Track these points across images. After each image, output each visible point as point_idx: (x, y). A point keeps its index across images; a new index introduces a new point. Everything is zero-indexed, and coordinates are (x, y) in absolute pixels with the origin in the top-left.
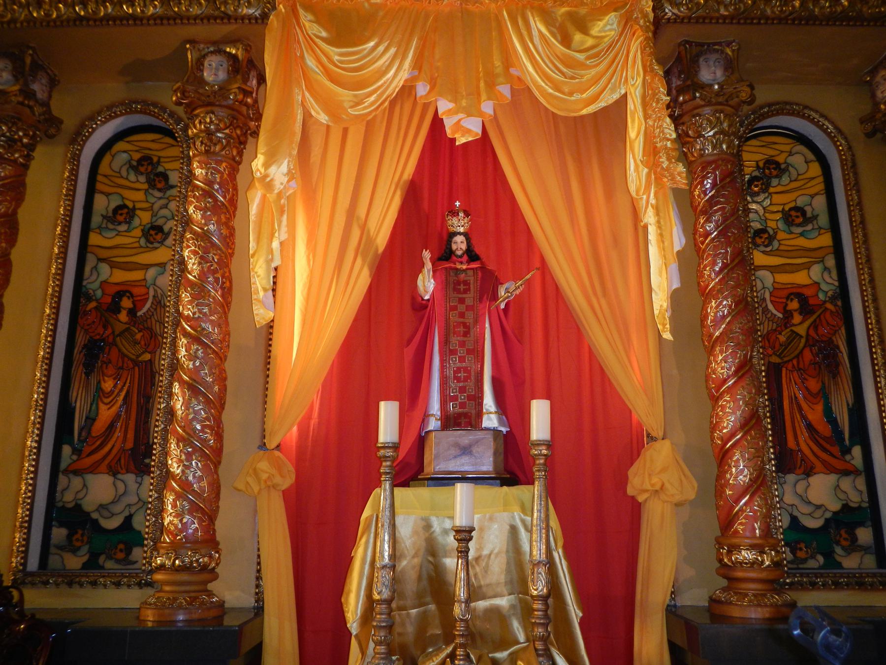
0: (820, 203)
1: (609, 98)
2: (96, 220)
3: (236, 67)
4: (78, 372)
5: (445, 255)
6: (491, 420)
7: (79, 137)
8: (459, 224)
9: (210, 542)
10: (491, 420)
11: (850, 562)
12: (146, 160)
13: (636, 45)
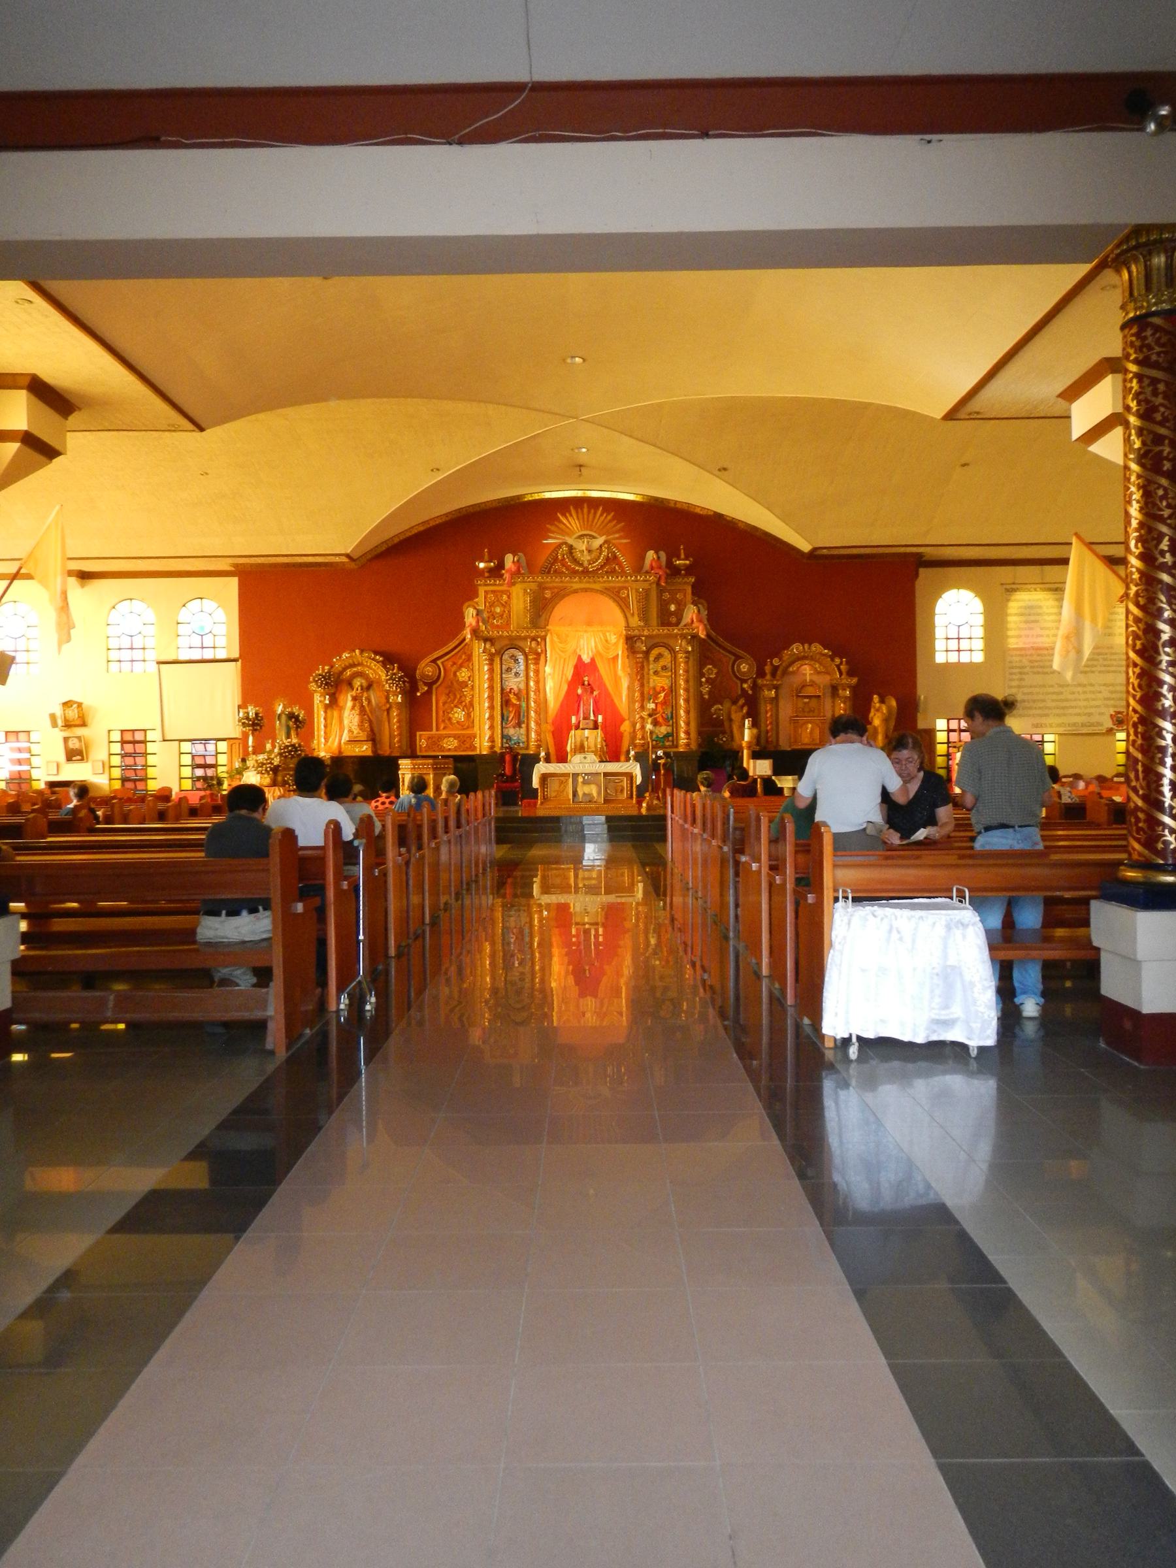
0: (670, 664)
1: (615, 654)
2: (503, 671)
3: (538, 644)
4: (504, 707)
5: (583, 685)
6: (592, 717)
7: (500, 652)
8: (586, 679)
9: (540, 741)
10: (592, 717)
11: (667, 744)
12: (513, 656)
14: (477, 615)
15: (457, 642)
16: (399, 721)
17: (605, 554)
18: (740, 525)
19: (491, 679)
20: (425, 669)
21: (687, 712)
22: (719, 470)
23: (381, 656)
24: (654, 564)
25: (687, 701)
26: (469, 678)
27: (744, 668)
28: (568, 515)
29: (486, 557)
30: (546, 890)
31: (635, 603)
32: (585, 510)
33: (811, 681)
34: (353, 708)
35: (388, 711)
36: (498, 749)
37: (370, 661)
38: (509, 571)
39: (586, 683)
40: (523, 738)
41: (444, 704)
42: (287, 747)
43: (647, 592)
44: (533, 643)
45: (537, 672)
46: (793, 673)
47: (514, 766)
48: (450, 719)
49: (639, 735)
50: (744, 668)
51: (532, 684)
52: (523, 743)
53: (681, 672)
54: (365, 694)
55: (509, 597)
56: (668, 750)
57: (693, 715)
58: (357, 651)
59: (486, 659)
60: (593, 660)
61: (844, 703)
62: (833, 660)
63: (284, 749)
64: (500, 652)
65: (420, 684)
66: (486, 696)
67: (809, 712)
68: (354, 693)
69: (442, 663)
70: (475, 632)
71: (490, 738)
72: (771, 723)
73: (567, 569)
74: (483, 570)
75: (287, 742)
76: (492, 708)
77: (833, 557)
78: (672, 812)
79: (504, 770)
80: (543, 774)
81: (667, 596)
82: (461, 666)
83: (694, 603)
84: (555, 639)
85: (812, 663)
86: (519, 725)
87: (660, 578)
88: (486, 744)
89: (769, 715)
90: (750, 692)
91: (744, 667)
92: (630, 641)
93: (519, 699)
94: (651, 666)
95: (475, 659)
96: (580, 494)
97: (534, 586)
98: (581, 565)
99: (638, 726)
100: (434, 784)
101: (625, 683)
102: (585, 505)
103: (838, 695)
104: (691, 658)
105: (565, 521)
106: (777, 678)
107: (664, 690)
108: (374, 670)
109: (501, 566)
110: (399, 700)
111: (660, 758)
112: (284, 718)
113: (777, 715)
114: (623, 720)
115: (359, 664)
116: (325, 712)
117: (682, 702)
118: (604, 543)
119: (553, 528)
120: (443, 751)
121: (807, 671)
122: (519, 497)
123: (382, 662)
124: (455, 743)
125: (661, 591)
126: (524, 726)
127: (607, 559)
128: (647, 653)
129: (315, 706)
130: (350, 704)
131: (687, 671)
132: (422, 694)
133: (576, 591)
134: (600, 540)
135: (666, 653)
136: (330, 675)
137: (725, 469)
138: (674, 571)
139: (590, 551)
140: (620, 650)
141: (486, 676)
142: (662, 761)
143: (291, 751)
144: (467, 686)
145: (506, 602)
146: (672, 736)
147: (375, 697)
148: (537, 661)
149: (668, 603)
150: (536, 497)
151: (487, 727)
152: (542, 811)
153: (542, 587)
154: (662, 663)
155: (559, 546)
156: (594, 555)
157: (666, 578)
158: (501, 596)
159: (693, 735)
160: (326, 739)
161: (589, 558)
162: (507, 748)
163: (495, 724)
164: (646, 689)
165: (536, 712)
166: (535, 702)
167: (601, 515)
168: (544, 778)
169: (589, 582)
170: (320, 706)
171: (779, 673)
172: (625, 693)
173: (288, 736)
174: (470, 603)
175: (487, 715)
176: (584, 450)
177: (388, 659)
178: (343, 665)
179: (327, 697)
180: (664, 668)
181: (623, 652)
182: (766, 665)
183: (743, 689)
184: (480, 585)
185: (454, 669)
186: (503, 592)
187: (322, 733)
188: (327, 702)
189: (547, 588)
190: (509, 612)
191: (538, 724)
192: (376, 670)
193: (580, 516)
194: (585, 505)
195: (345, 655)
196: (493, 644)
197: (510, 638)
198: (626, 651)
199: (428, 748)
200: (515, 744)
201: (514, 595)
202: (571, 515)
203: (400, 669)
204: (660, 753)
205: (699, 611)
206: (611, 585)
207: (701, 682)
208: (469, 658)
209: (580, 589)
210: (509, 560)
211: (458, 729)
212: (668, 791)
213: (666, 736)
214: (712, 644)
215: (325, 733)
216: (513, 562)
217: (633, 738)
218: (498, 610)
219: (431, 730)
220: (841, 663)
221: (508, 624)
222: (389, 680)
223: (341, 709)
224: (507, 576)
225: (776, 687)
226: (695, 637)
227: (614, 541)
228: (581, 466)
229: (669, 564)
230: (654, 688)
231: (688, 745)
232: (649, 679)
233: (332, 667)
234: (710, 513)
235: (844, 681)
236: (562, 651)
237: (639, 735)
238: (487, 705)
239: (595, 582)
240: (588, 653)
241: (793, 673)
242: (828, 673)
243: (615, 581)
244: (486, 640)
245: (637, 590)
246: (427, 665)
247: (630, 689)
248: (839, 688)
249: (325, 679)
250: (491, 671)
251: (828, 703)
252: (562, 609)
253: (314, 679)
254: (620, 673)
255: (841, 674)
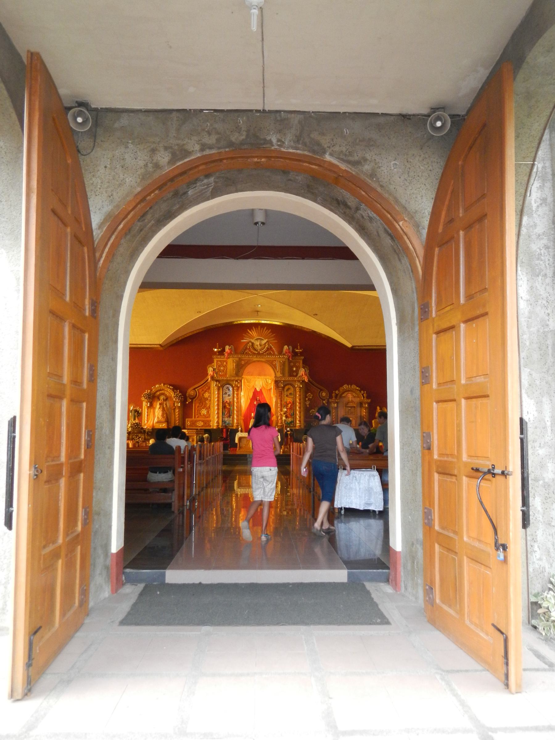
3: (238, 383)
5: (257, 400)
8: (258, 398)
9: (238, 423)
12: (228, 388)
13: (273, 382)
14: (213, 370)
15: (204, 381)
16: (178, 414)
17: (267, 346)
18: (323, 335)
19: (218, 397)
20: (191, 392)
21: (300, 412)
22: (314, 315)
23: (172, 387)
24: (287, 351)
25: (300, 408)
26: (209, 396)
27: (324, 394)
28: (252, 330)
29: (217, 347)
30: (240, 486)
31: (279, 366)
32: (259, 328)
33: (352, 400)
34: (160, 408)
35: (174, 409)
36: (220, 427)
37: (167, 388)
38: (227, 352)
39: (258, 399)
40: (231, 422)
41: (198, 407)
42: (134, 424)
43: (284, 363)
44: (236, 383)
45: (237, 394)
46: (344, 397)
47: (227, 433)
48: (200, 413)
49: (280, 422)
50: (324, 394)
51: (235, 399)
52: (231, 424)
53: (298, 396)
54: (165, 402)
55: (226, 363)
56: (292, 428)
57: (302, 413)
58: (162, 384)
59: (216, 389)
60: (261, 390)
61: (365, 410)
62: (360, 392)
63: (133, 424)
64: (222, 386)
65: (188, 398)
66: (216, 404)
67: (351, 413)
68: (160, 402)
69: (198, 390)
70: (212, 378)
71: (217, 422)
72: (335, 418)
73: (251, 352)
74: (216, 352)
75: (134, 422)
76: (218, 409)
77: (360, 349)
78: (293, 452)
79: (223, 435)
80: (240, 437)
81: (292, 364)
82: (206, 391)
83: (303, 367)
84: (246, 381)
85: (352, 393)
86: (229, 416)
87: (289, 357)
88: (215, 424)
89: (334, 414)
90: (326, 405)
91: (324, 394)
92: (277, 382)
93: (230, 406)
94: (285, 393)
95: (212, 388)
96: (257, 322)
97: (237, 359)
98: (257, 351)
99: (279, 418)
100: (196, 440)
101: (274, 400)
102: (259, 327)
103: (363, 407)
104: (302, 389)
105: (251, 333)
106: (338, 399)
107: (290, 403)
108: (169, 392)
109: (224, 350)
110: (179, 405)
111: (288, 431)
112: (133, 411)
113: (337, 414)
114: (273, 415)
115: (163, 390)
116: (148, 410)
117: (298, 408)
118: (266, 342)
119: (246, 336)
120: (197, 427)
121: (350, 396)
122: (232, 322)
123: (172, 389)
124: (202, 424)
125: (290, 362)
126: (231, 417)
127: (268, 348)
128: (283, 388)
129: (143, 407)
130: (158, 406)
131: (300, 395)
132: (189, 403)
133: (254, 362)
134: (265, 341)
135: (291, 388)
136: (150, 394)
137: (316, 315)
138: (295, 354)
139: (260, 345)
140: (272, 386)
141: (216, 396)
142: (289, 433)
143: (136, 426)
144: (208, 400)
145: (225, 365)
146: (293, 422)
147: (168, 404)
148: (238, 390)
149: (292, 367)
150: (239, 322)
151: (216, 417)
152: (238, 452)
153: (240, 360)
154: (289, 392)
155: (248, 343)
156: (263, 346)
157: (292, 357)
158: (224, 363)
159: (302, 422)
160: (148, 421)
161: (260, 348)
162: (224, 426)
163: (219, 416)
164: (283, 403)
165: (237, 411)
166: (236, 407)
167: (266, 331)
168: (240, 439)
169: (260, 358)
170: (145, 407)
171: (338, 397)
172: (274, 404)
173: (134, 419)
174: (211, 365)
175: (216, 412)
176: (260, 306)
177: (175, 388)
178: (156, 390)
179: (149, 403)
180: (291, 394)
181: (273, 387)
182: (333, 393)
183: (323, 403)
184: (215, 358)
185: (202, 393)
186: (224, 361)
187: (146, 418)
188: (149, 405)
189: (242, 360)
190: (227, 369)
191: (237, 416)
192: (170, 392)
193: (257, 331)
194: (259, 327)
195: (157, 386)
196: (219, 383)
197: (227, 380)
198: (275, 387)
199: (190, 425)
200: (227, 424)
201: (229, 363)
202: (253, 330)
203: (180, 392)
204: (288, 429)
205: (305, 371)
206: (269, 359)
207: (306, 400)
208: (209, 388)
209: (257, 361)
210: (227, 348)
211: (203, 418)
212: (291, 444)
213: (291, 422)
214: (311, 384)
215: (147, 418)
216: (229, 349)
217: (277, 423)
218: (222, 368)
219: (192, 418)
220: (364, 393)
221: (226, 374)
222: (175, 396)
223: (154, 409)
224: (226, 355)
225: (337, 403)
226: (303, 381)
227: (271, 341)
228: (258, 311)
229: (293, 351)
230: (286, 402)
231: (300, 426)
232: (284, 398)
233: (151, 391)
234: (310, 331)
235: (365, 401)
236: (248, 386)
237: (280, 422)
238: (216, 408)
239: (262, 358)
240: (259, 387)
241: (344, 397)
242: (358, 397)
243: (271, 358)
244: (217, 381)
245: (280, 362)
246: (191, 391)
247: (276, 402)
248: (363, 403)
249: (148, 396)
250: (218, 394)
251: (359, 409)
252: (249, 368)
253: (144, 396)
254: (272, 395)
255: (364, 397)
